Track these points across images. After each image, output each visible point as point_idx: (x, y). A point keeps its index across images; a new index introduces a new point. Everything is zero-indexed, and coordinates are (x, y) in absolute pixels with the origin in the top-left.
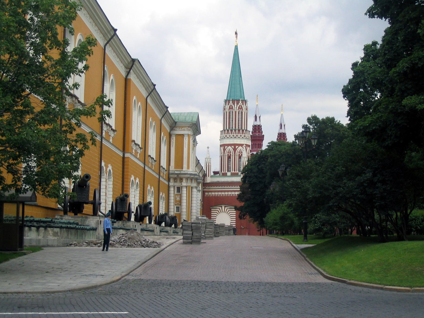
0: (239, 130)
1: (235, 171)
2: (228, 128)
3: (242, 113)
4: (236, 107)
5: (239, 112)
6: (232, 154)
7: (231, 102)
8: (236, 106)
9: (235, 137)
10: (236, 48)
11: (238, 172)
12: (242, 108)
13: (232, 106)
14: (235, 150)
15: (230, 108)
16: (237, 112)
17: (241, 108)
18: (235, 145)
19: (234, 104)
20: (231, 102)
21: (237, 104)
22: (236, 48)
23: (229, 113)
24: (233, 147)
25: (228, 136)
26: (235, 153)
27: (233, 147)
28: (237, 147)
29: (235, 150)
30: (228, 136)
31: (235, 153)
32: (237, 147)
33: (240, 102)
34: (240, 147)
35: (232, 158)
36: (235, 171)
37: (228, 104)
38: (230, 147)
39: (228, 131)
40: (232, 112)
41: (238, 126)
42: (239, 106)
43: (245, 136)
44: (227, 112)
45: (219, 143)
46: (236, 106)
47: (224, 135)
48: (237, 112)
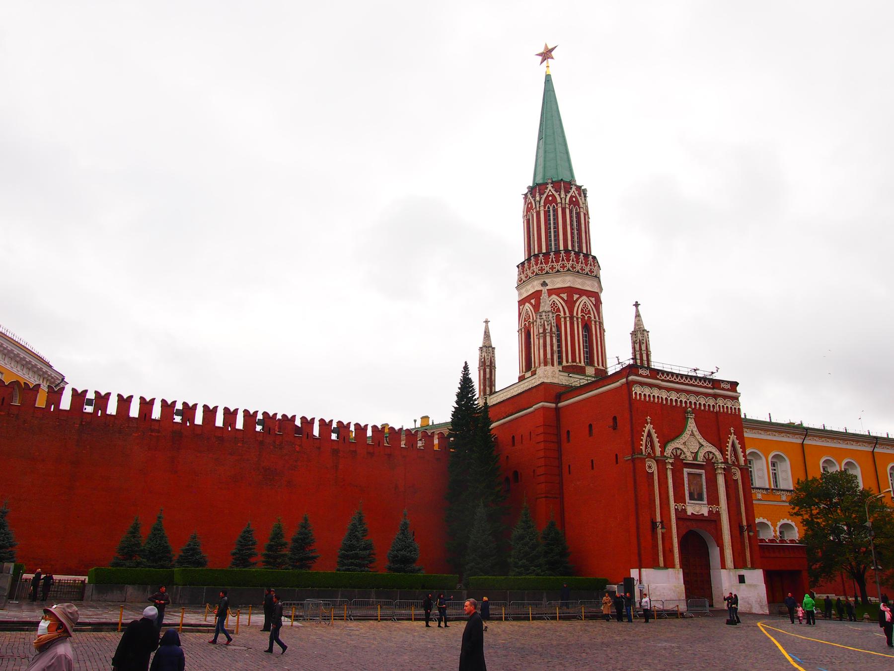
0: (577, 254)
1: (574, 360)
2: (544, 251)
3: (578, 214)
4: (563, 198)
5: (571, 212)
6: (562, 314)
7: (550, 187)
8: (563, 196)
9: (569, 270)
10: (548, 80)
11: (583, 364)
12: (576, 203)
13: (553, 196)
14: (571, 304)
15: (547, 201)
16: (568, 211)
17: (574, 202)
18: (571, 291)
19: (558, 190)
20: (550, 187)
21: (567, 192)
22: (548, 80)
23: (547, 213)
24: (565, 296)
25: (547, 269)
26: (571, 312)
27: (565, 296)
28: (576, 297)
29: (571, 304)
30: (547, 269)
31: (571, 312)
32: (576, 297)
33: (574, 188)
34: (584, 298)
35: (565, 328)
36: (574, 360)
37: (541, 194)
38: (554, 297)
39: (547, 255)
40: (555, 211)
41: (573, 242)
42: (572, 197)
43: (591, 272)
44: (538, 214)
45: (515, 297)
46: (563, 196)
47: (536, 269)
48: (568, 211)
